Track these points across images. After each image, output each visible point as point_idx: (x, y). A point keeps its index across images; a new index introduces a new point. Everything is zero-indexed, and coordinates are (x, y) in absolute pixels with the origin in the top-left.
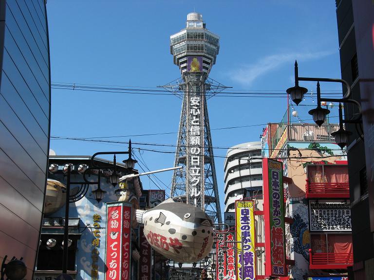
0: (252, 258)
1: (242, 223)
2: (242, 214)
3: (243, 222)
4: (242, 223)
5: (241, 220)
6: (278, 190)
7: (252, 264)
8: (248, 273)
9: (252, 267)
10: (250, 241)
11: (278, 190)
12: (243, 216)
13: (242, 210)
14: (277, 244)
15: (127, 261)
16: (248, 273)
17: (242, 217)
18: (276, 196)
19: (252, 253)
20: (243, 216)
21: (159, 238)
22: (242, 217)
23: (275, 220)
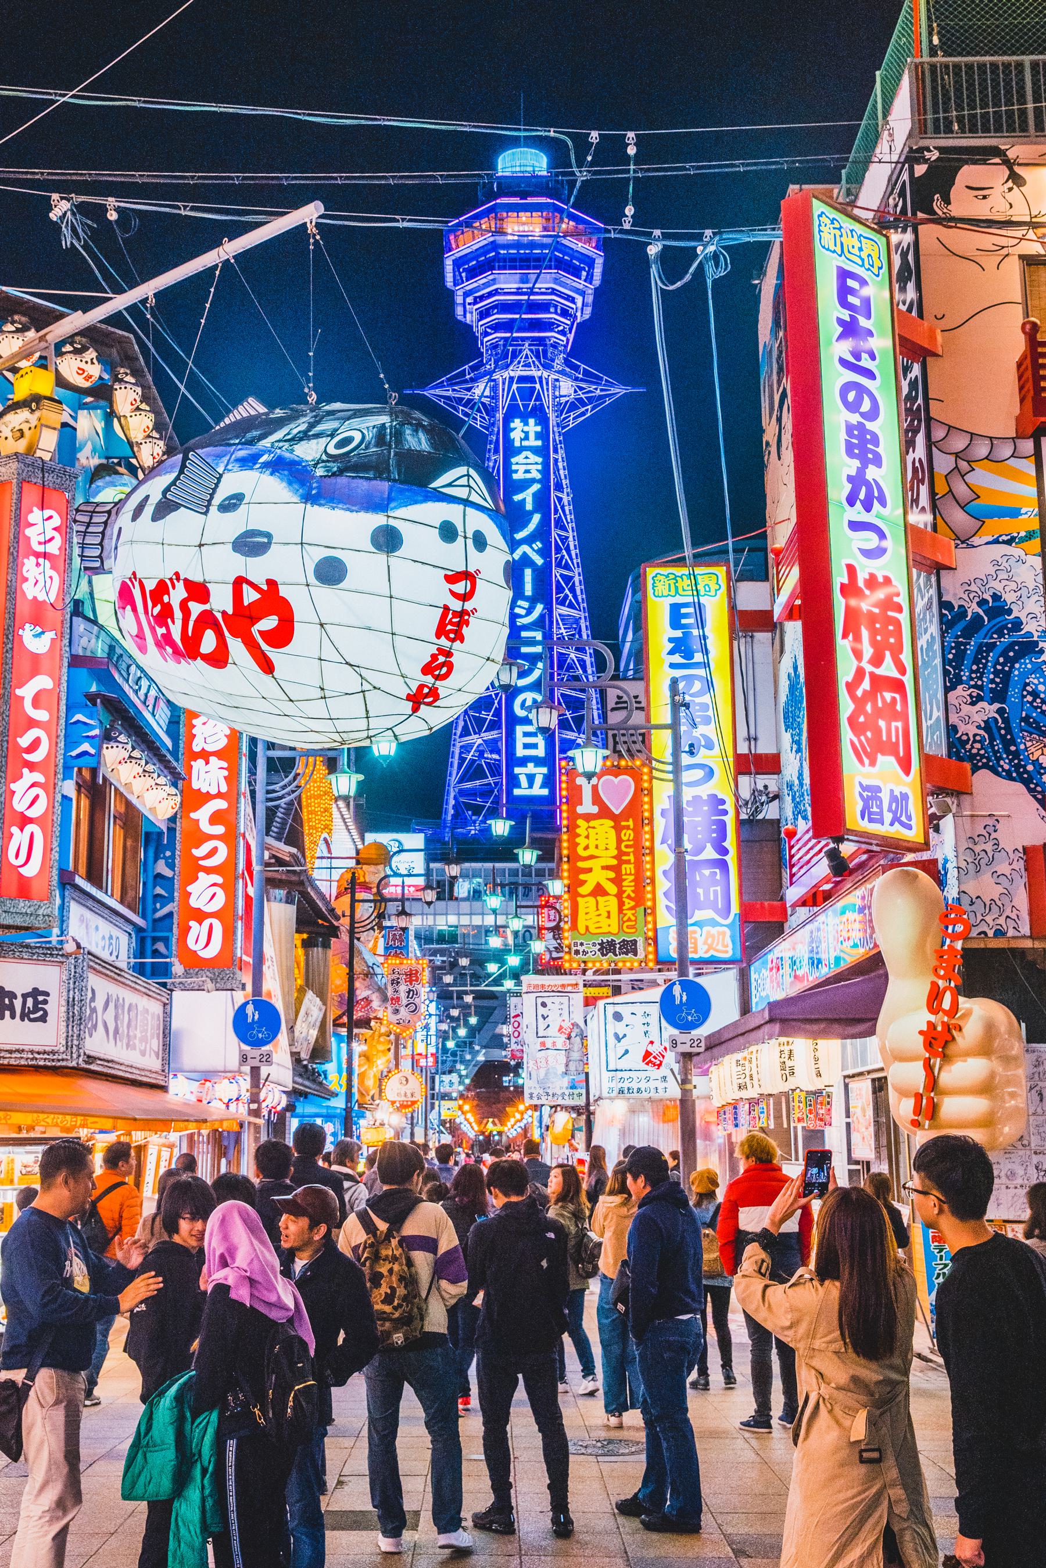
0: (722, 826)
1: (672, 666)
2: (675, 624)
3: (677, 659)
4: (672, 666)
5: (671, 652)
6: (870, 374)
7: (725, 851)
8: (707, 894)
9: (723, 865)
10: (709, 746)
11: (870, 374)
12: (678, 634)
13: (675, 608)
14: (877, 660)
15: (38, 777)
16: (707, 894)
17: (671, 640)
18: (859, 401)
19: (723, 802)
20: (678, 634)
21: (177, 595)
22: (671, 640)
23: (855, 526)
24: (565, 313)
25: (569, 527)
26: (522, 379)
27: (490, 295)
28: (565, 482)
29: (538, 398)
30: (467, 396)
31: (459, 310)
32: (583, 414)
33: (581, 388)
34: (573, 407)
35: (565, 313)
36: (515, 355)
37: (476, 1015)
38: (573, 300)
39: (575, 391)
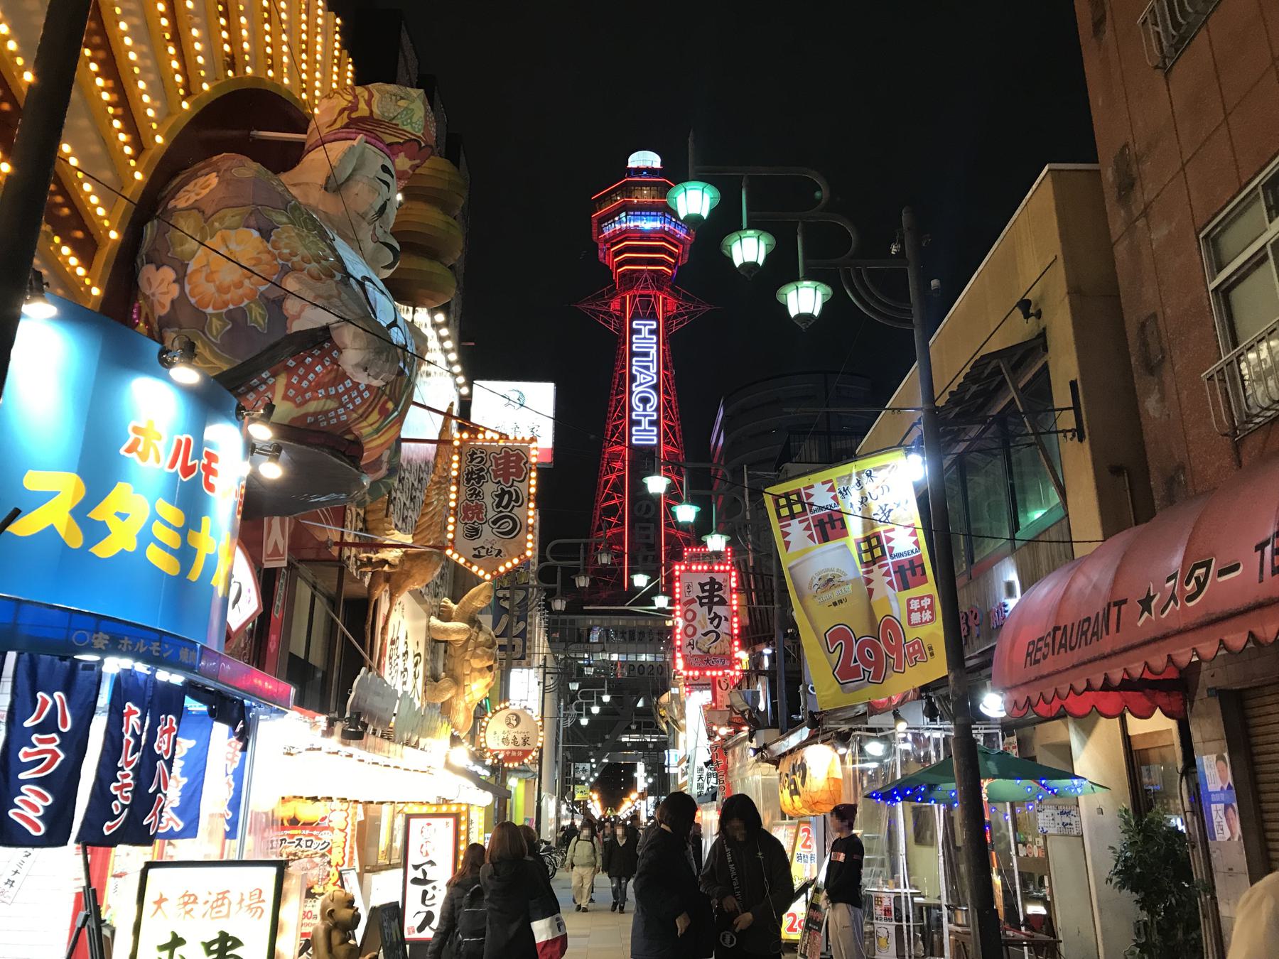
24: (671, 254)
25: (672, 394)
26: (641, 296)
27: (621, 241)
28: (670, 365)
29: (653, 308)
30: (605, 309)
31: (601, 255)
32: (681, 323)
33: (682, 306)
34: (675, 317)
35: (671, 254)
36: (637, 280)
37: (608, 694)
38: (676, 247)
39: (677, 308)
